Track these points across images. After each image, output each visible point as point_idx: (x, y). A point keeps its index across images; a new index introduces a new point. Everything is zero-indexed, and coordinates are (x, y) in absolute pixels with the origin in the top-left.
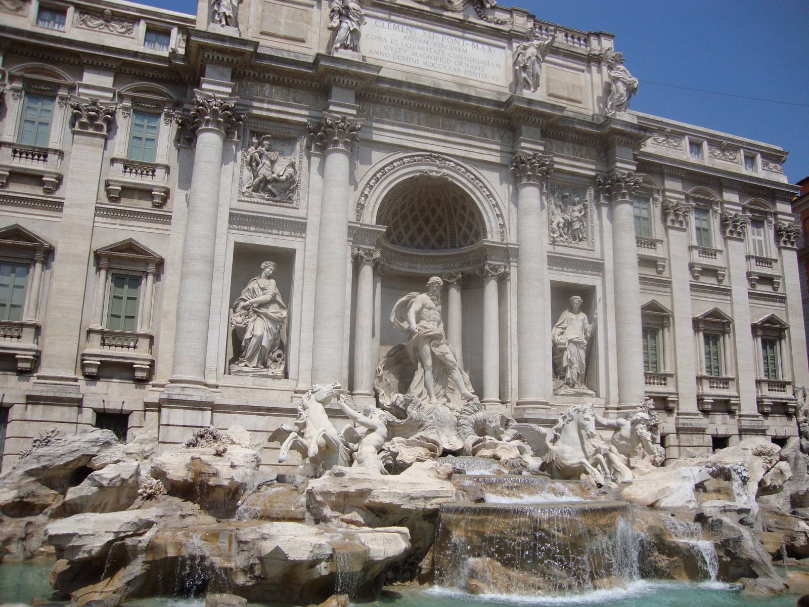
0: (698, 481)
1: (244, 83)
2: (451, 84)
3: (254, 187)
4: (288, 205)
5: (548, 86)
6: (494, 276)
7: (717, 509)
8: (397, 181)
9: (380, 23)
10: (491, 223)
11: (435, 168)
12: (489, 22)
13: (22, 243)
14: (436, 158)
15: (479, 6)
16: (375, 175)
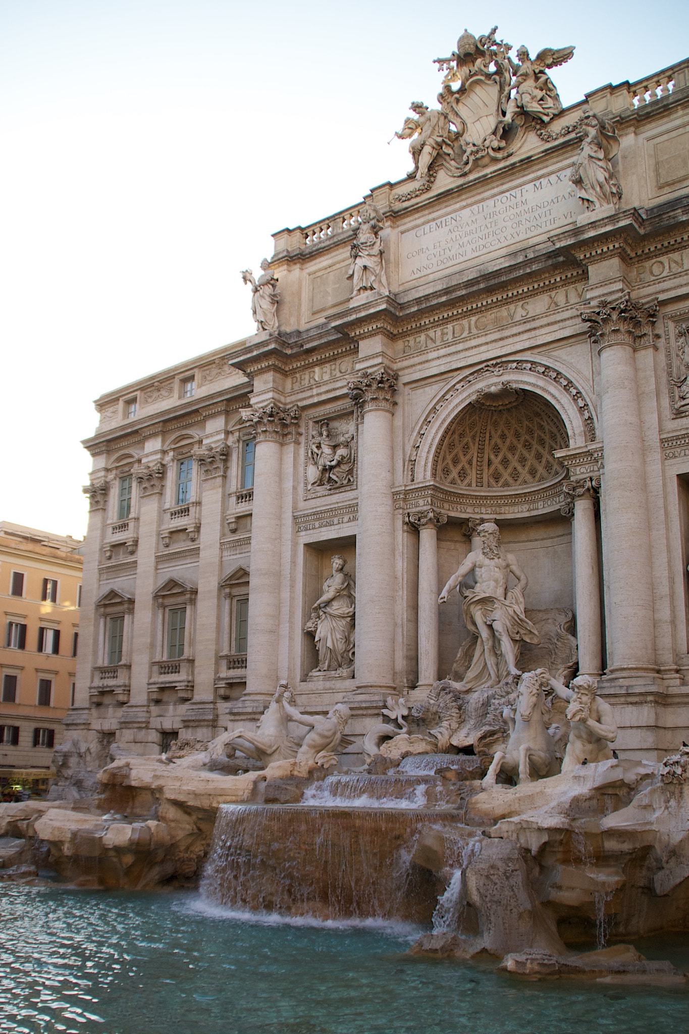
0: (597, 785)
1: (298, 375)
2: (502, 260)
3: (321, 480)
4: (348, 488)
5: (658, 175)
6: (579, 496)
7: (513, 827)
8: (452, 416)
9: (420, 231)
10: (573, 421)
11: (495, 380)
12: (556, 139)
13: (175, 592)
14: (494, 366)
15: (538, 127)
16: (426, 420)
